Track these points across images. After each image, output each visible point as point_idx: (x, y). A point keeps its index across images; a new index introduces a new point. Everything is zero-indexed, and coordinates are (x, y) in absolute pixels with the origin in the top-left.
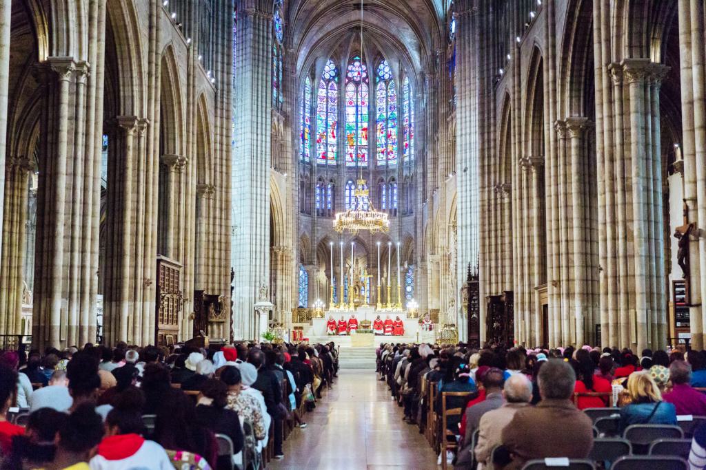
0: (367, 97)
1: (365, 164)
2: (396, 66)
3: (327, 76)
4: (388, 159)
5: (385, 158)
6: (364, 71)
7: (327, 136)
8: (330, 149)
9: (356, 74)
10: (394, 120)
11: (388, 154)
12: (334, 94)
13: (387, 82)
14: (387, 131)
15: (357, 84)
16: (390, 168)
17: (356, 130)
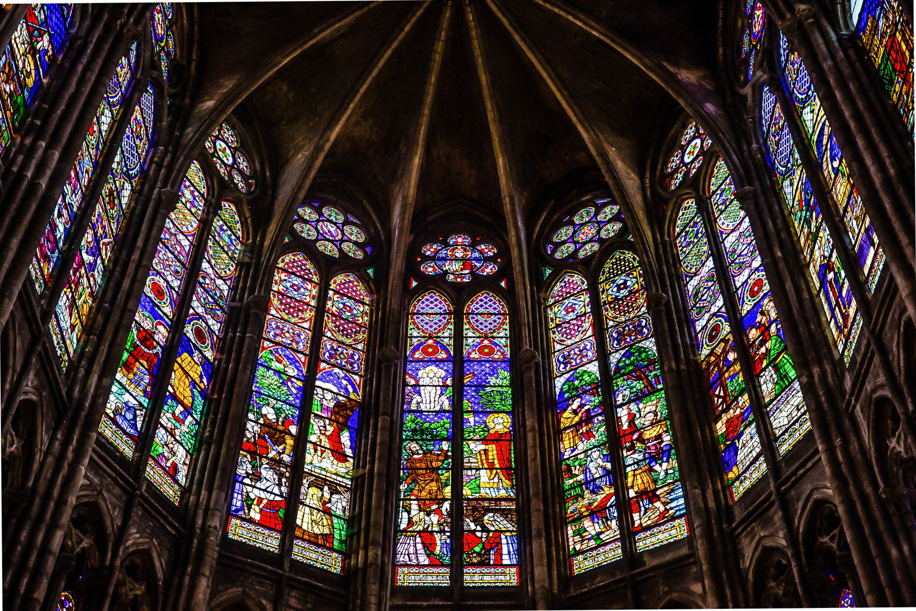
0: (505, 331)
1: (510, 578)
2: (631, 181)
3: (328, 249)
4: (628, 534)
5: (614, 529)
6: (492, 259)
7: (301, 440)
8: (311, 495)
9: (456, 266)
10: (638, 372)
11: (625, 507)
12: (361, 313)
13: (591, 269)
14: (612, 422)
15: (459, 296)
16: (650, 562)
17: (457, 437)
